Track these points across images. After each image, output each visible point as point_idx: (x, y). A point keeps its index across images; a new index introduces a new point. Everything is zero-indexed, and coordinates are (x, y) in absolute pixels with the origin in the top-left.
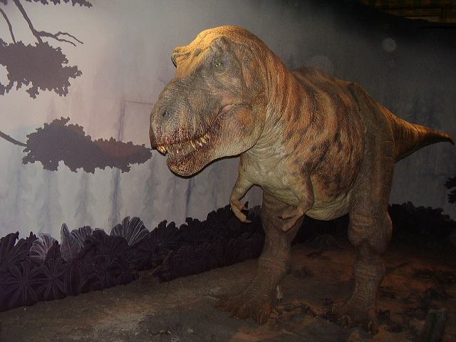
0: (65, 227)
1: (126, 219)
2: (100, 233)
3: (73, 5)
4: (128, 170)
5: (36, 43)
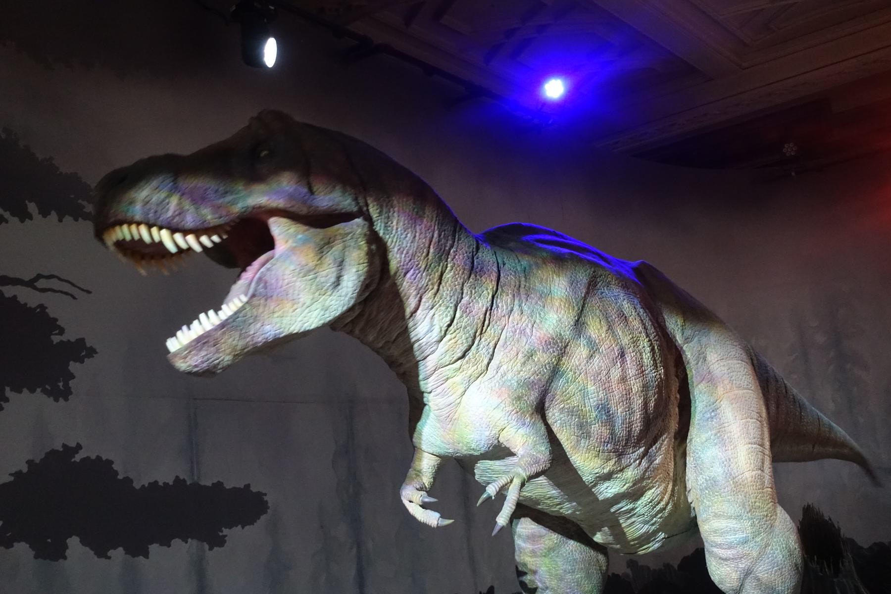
3: (60, 221)
4: (220, 542)
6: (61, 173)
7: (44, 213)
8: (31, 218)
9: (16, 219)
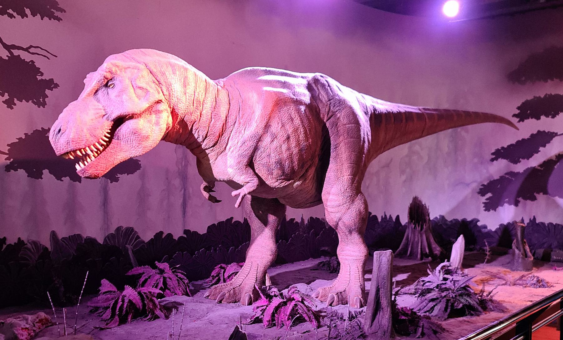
0: (54, 234)
1: (118, 229)
2: (91, 241)
5: (7, 56)
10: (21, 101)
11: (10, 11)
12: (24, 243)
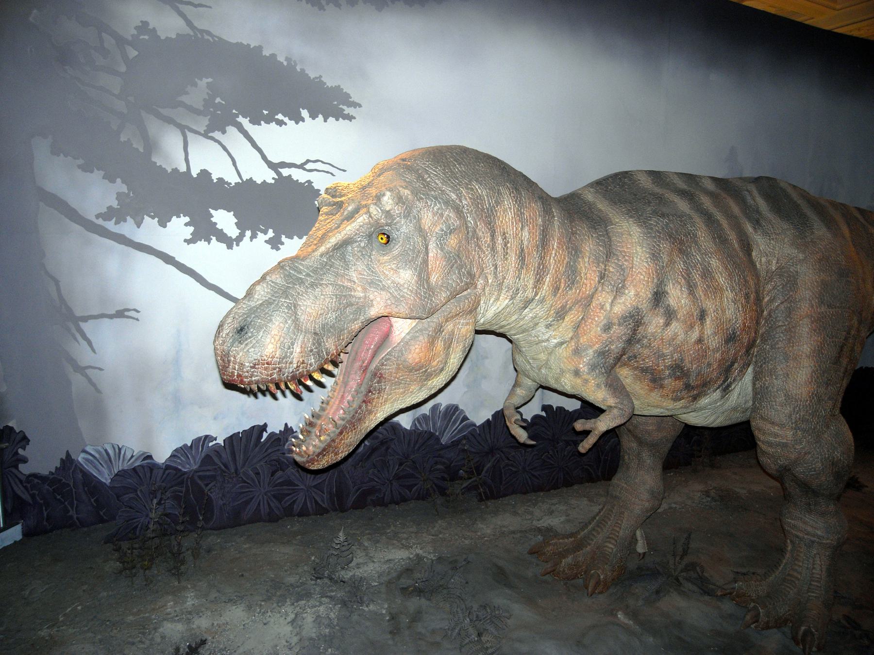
3: (325, 121)
5: (273, 178)
6: (328, 86)
7: (313, 116)
8: (303, 120)
9: (293, 122)
10: (292, 238)
11: (280, 117)
12: (293, 430)
